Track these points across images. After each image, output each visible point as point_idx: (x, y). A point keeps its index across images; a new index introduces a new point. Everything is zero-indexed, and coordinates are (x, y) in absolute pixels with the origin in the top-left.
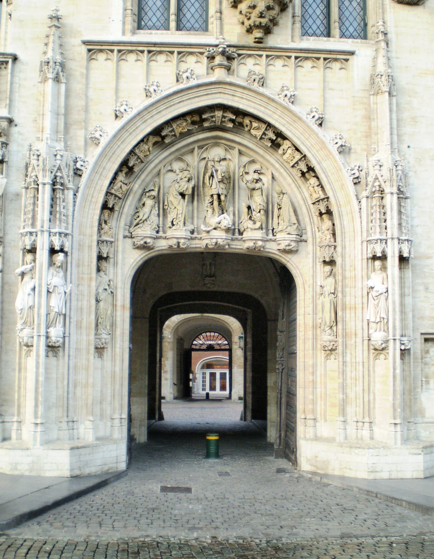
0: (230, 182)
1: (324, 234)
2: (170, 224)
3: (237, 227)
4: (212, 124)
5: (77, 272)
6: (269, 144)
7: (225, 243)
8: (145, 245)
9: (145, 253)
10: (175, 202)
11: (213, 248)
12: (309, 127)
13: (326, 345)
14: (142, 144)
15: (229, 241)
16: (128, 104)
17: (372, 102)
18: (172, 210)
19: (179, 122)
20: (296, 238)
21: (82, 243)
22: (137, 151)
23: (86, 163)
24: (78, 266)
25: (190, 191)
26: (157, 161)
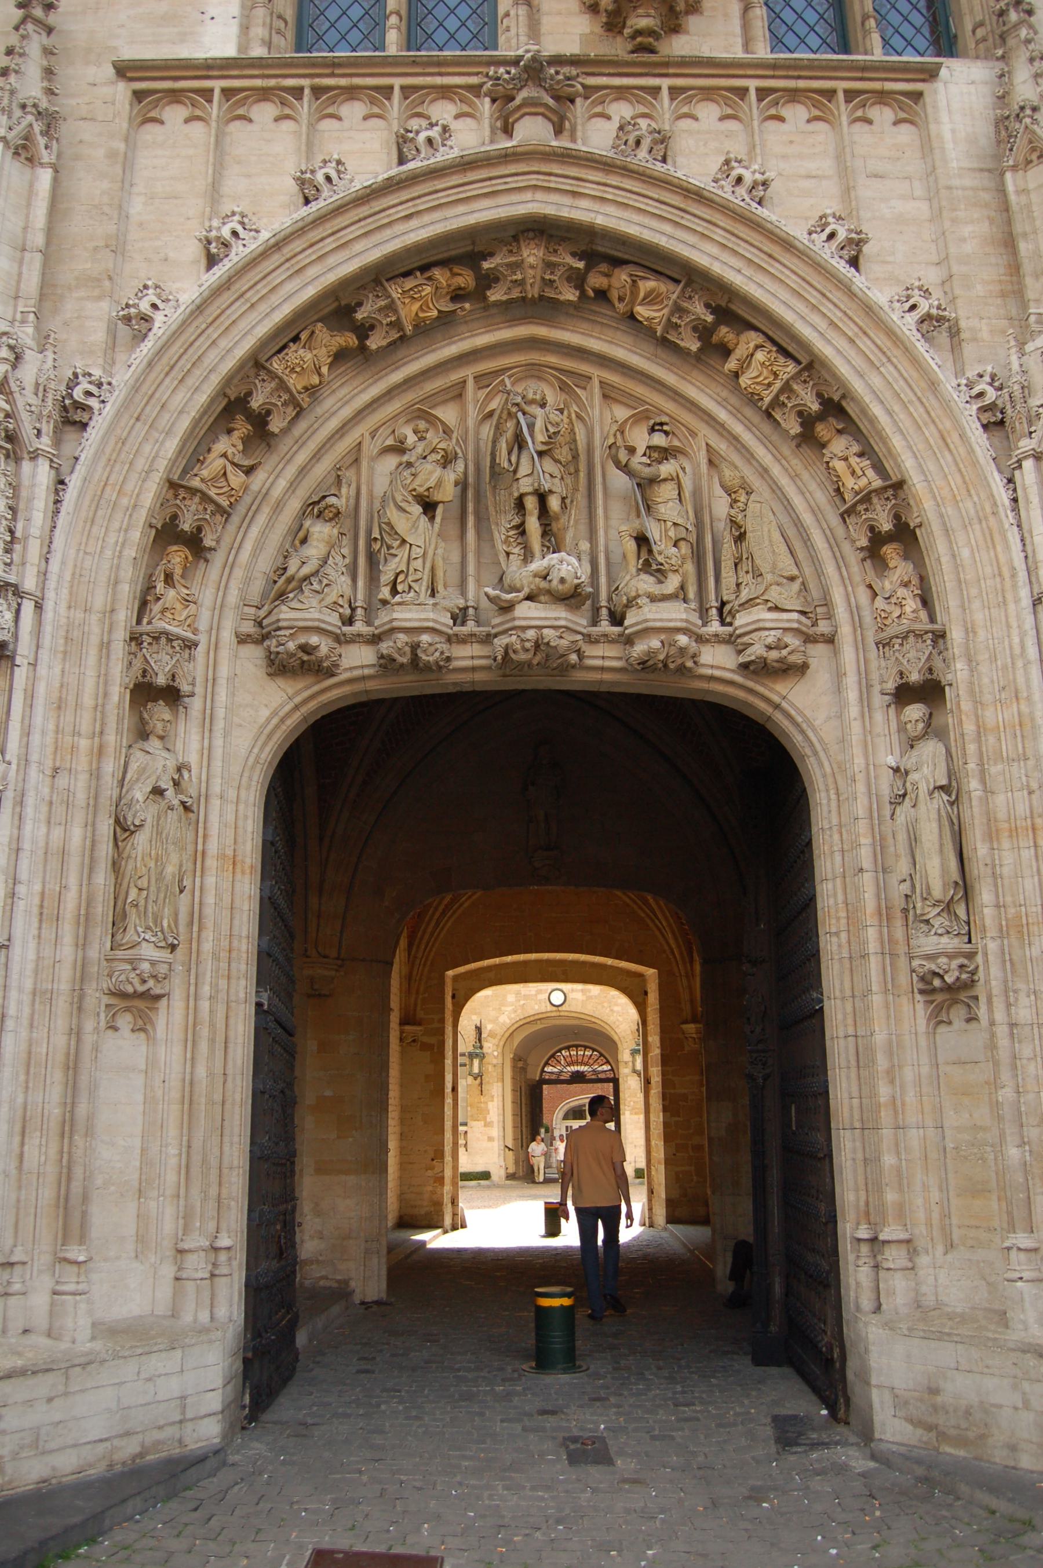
0: (577, 471)
1: (893, 600)
2: (385, 592)
3: (604, 603)
4: (515, 294)
5: (51, 726)
6: (694, 346)
7: (564, 643)
8: (306, 658)
9: (307, 688)
10: (401, 524)
11: (529, 664)
12: (819, 267)
13: (933, 967)
14: (293, 347)
15: (579, 637)
16: (246, 220)
17: (1010, 188)
18: (392, 551)
19: (409, 283)
20: (799, 622)
21: (76, 634)
22: (276, 365)
23: (105, 387)
24: (60, 706)
25: (448, 493)
26: (347, 412)
